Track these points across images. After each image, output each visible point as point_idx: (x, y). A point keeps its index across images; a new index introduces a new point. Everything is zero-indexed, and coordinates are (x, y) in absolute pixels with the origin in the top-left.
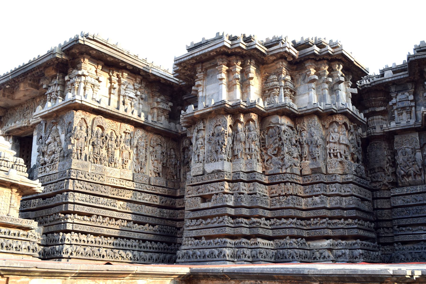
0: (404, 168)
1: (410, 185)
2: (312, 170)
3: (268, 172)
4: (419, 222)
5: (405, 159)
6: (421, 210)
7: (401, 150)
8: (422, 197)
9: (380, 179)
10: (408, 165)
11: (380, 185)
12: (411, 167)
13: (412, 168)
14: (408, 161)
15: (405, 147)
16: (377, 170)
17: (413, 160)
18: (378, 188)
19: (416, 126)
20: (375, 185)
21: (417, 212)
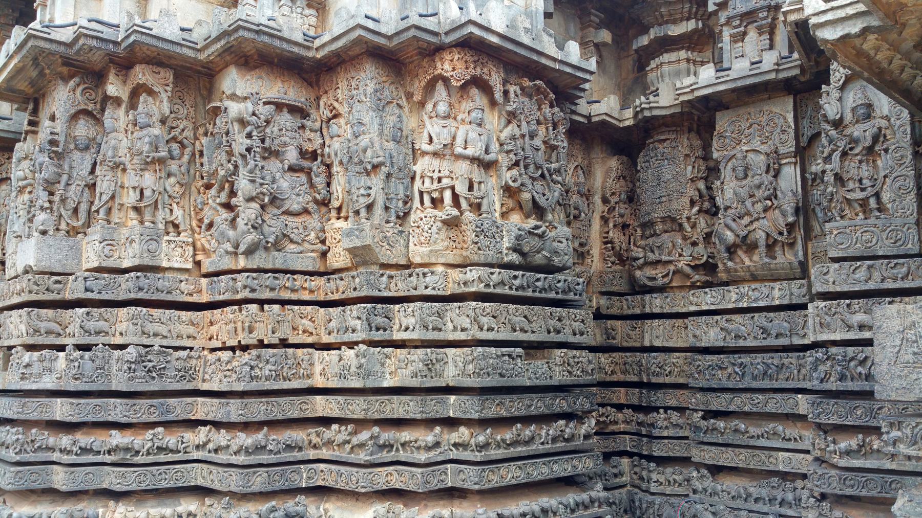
0: (734, 220)
1: (754, 278)
2: (352, 251)
3: (208, 266)
4: (770, 408)
5: (743, 192)
6: (780, 367)
7: (734, 160)
8: (785, 324)
9: (669, 254)
10: (749, 211)
11: (667, 275)
12: (758, 219)
13: (761, 221)
14: (751, 196)
15: (745, 148)
16: (659, 227)
17: (767, 193)
18: (660, 282)
19: (781, 76)
20: (654, 272)
21: (765, 373)
